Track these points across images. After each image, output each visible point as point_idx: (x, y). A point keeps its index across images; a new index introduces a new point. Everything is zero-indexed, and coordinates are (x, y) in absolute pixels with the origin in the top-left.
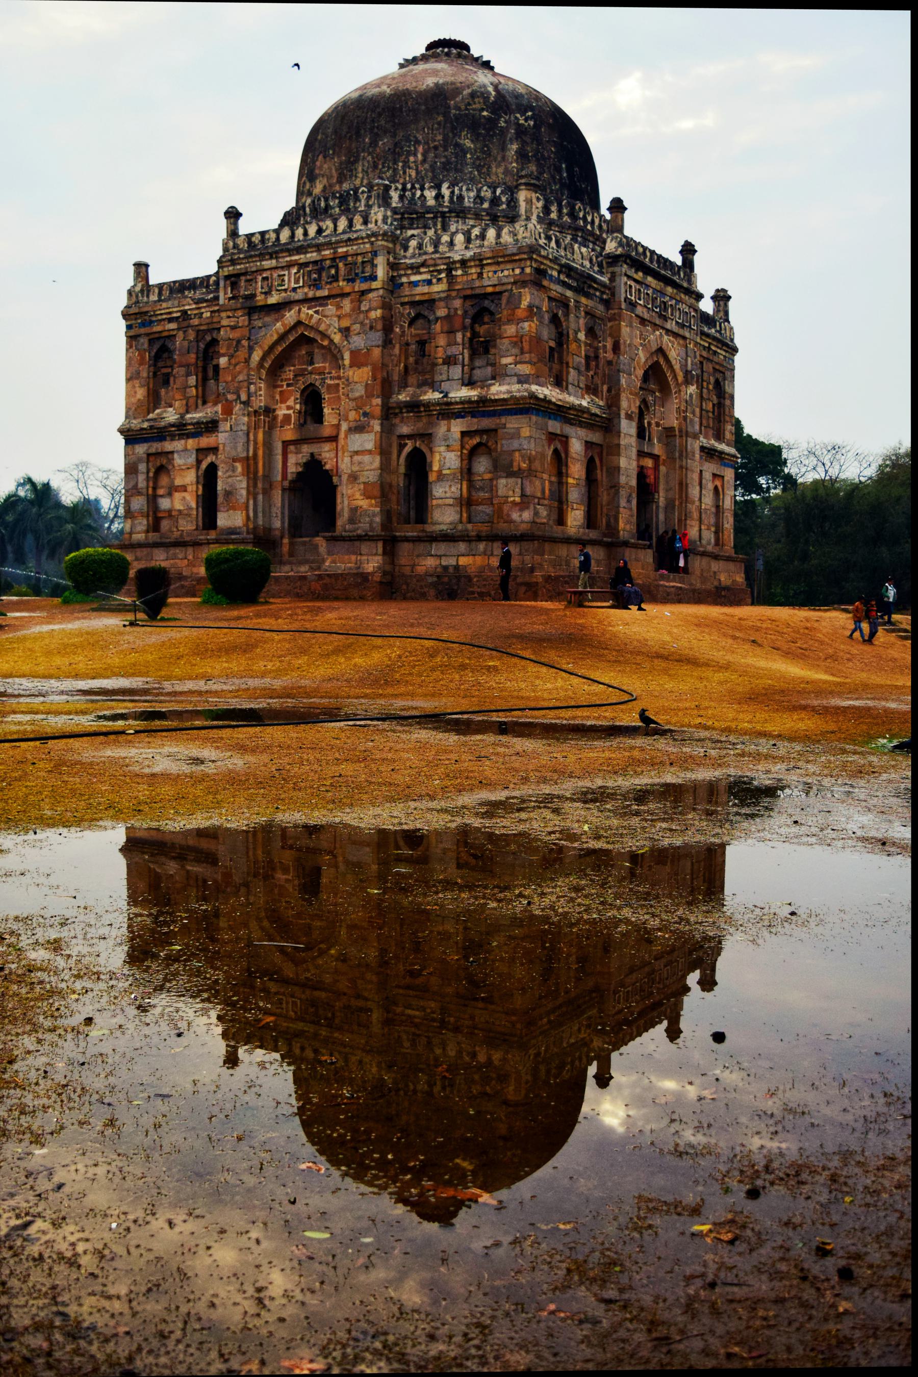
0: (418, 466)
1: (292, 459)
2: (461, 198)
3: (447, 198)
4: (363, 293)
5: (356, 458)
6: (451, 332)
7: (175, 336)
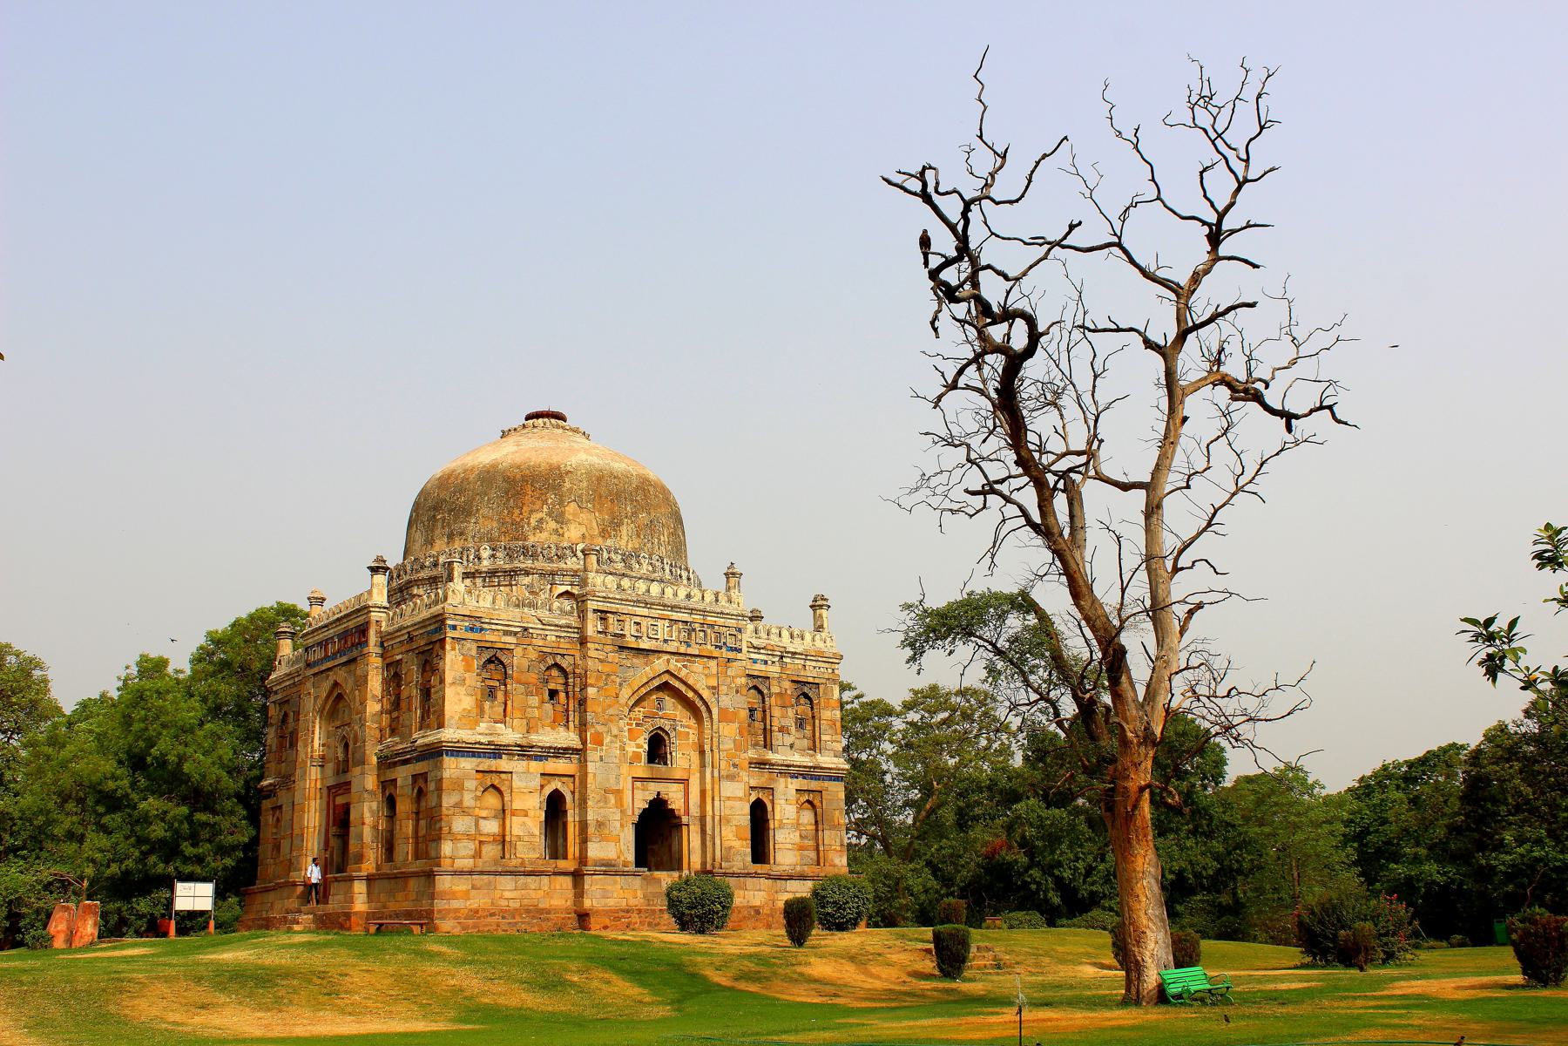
1: (639, 795)
5: (728, 803)
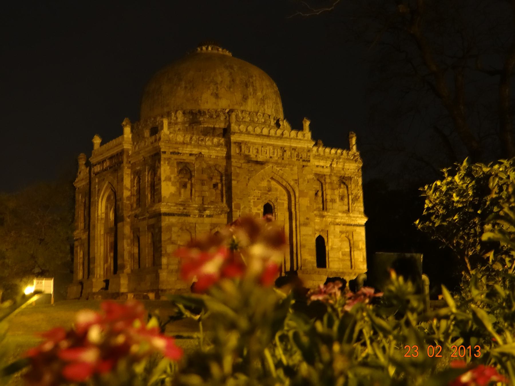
4: (303, 166)
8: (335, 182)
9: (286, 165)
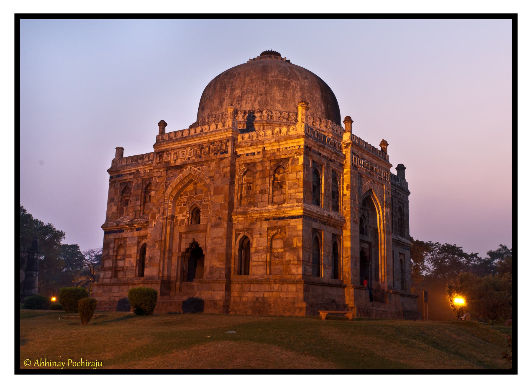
0: (245, 246)
1: (184, 241)
2: (271, 117)
3: (265, 117)
4: (221, 159)
5: (214, 240)
6: (264, 178)
7: (132, 182)
8: (268, 168)
9: (204, 162)
